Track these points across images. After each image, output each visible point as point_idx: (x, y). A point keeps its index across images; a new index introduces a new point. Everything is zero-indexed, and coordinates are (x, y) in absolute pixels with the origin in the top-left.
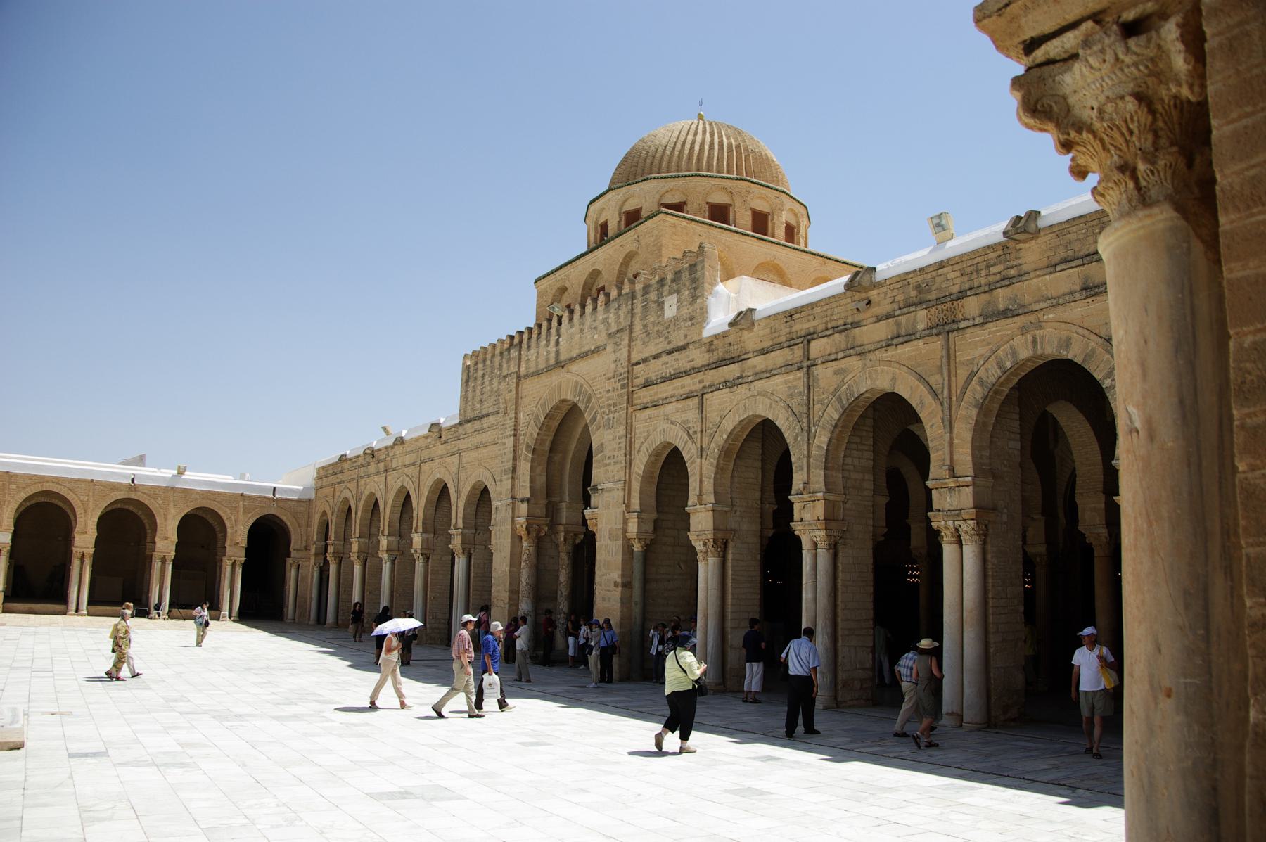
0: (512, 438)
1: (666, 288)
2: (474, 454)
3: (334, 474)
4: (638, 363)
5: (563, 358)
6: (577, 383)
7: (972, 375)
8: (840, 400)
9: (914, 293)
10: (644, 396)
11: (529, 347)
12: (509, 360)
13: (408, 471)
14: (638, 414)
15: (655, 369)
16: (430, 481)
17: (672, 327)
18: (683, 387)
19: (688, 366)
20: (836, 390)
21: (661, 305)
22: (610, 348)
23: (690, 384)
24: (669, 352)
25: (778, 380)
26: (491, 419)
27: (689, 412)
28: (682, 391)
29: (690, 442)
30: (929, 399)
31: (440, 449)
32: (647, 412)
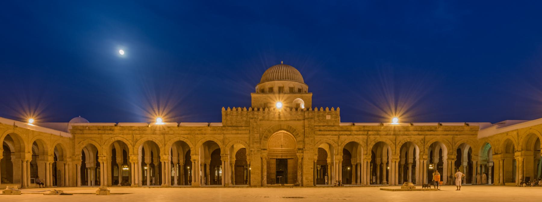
0: (258, 135)
2: (232, 136)
3: (99, 130)
6: (289, 126)
12: (253, 114)
13: (186, 136)
15: (322, 128)
16: (204, 141)
21: (325, 116)
22: (306, 121)
25: (361, 136)
26: (244, 128)
27: (336, 138)
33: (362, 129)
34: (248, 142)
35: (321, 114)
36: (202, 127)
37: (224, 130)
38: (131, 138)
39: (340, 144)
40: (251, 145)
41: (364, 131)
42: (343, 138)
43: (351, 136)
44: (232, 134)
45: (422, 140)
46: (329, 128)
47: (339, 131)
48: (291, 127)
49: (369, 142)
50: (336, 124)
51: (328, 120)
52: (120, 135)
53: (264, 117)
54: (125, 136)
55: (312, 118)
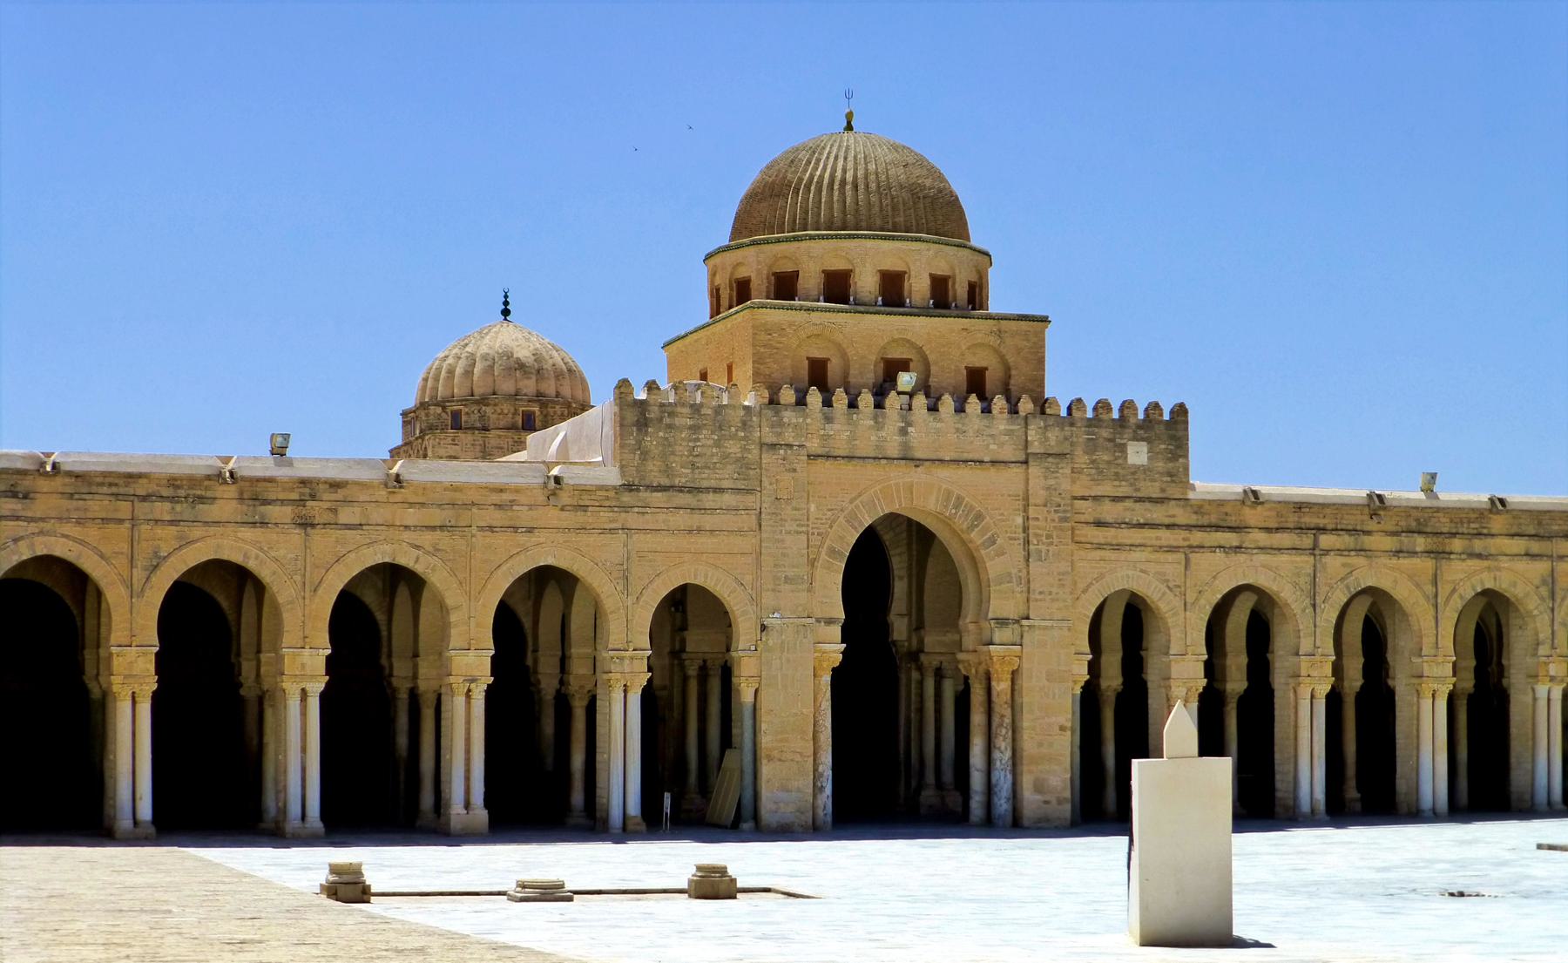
0: (804, 537)
1: (1128, 433)
4: (1083, 498)
5: (918, 455)
6: (949, 493)
7: (1454, 590)
8: (1348, 587)
9: (1414, 524)
10: (1100, 535)
11: (829, 419)
13: (427, 538)
14: (1082, 553)
15: (1109, 511)
17: (1140, 475)
18: (1158, 538)
19: (1167, 521)
20: (1342, 579)
21: (1122, 448)
22: (1035, 470)
23: (1167, 537)
24: (1140, 500)
25: (1284, 558)
26: (728, 499)
27: (1172, 565)
28: (1158, 543)
29: (1170, 595)
30: (1422, 601)
31: (552, 516)
32: (1099, 553)
33: (1292, 520)
34: (748, 579)
35: (1105, 433)
36: (517, 491)
37: (626, 508)
38: (125, 547)
39: (1190, 598)
40: (768, 599)
41: (1301, 529)
42: (1204, 562)
43: (1242, 557)
44: (671, 532)
45: (1544, 582)
46: (1141, 513)
47: (1189, 527)
48: (959, 499)
49: (1322, 590)
50: (1173, 491)
51: (1136, 470)
52: (68, 529)
53: (826, 438)
54: (92, 533)
55: (1062, 455)
